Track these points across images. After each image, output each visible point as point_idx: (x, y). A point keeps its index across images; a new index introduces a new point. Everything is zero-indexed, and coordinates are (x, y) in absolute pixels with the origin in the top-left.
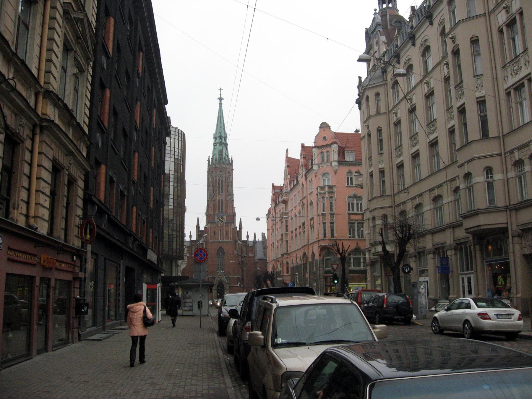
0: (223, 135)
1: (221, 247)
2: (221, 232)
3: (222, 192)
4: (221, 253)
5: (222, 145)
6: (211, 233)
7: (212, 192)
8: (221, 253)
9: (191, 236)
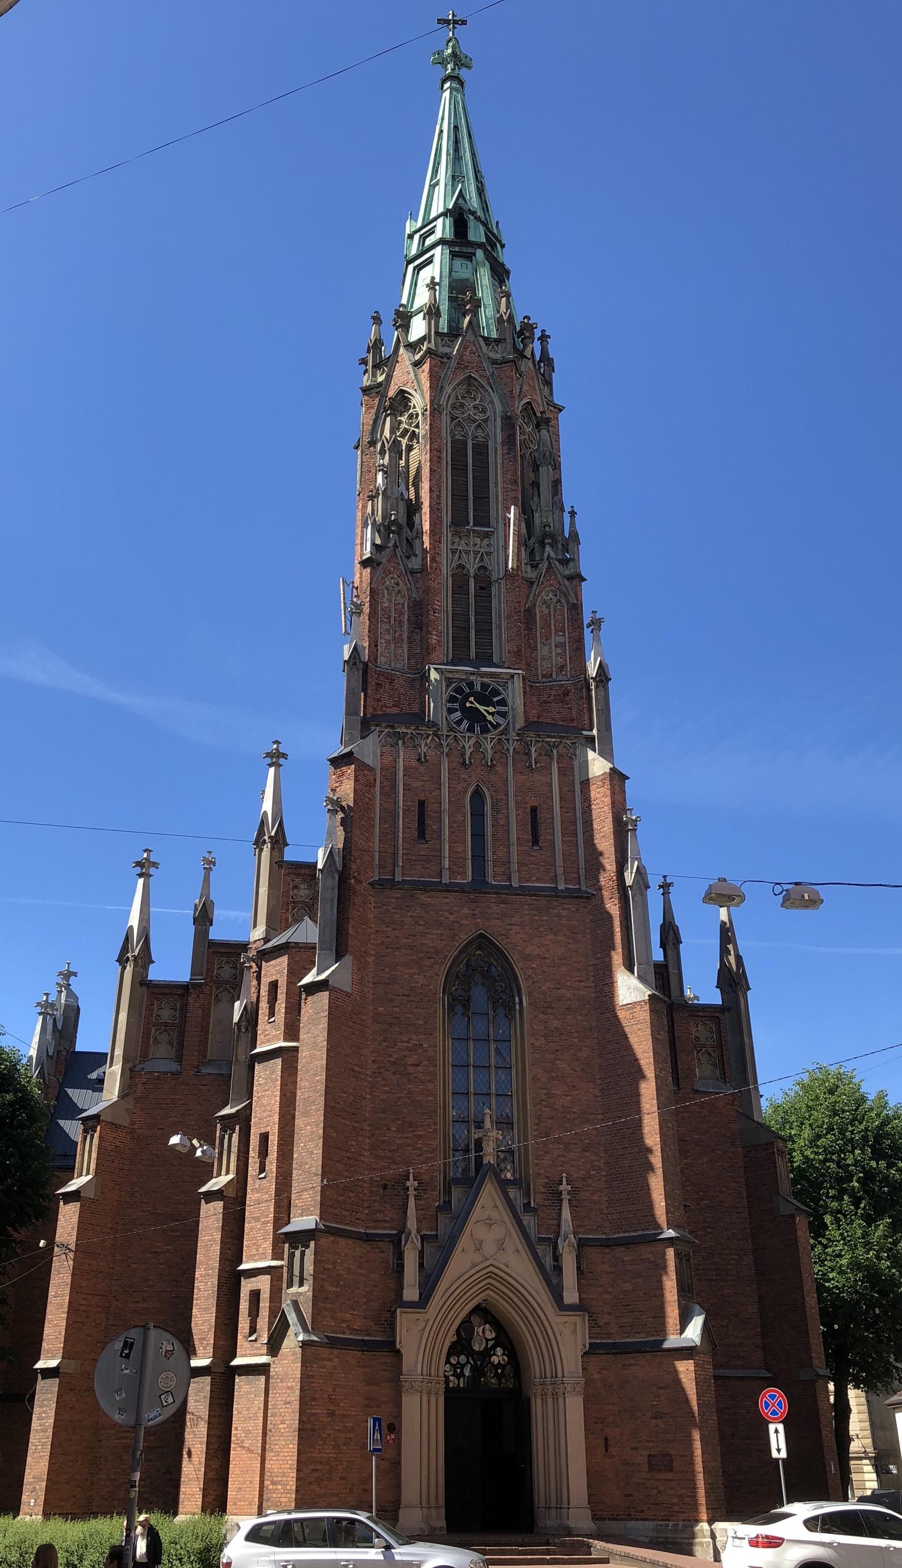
0: (474, 202)
1: (482, 941)
2: (478, 815)
3: (483, 519)
4: (479, 995)
5: (469, 257)
6: (389, 817)
7: (402, 520)
8: (479, 995)
9: (203, 917)
